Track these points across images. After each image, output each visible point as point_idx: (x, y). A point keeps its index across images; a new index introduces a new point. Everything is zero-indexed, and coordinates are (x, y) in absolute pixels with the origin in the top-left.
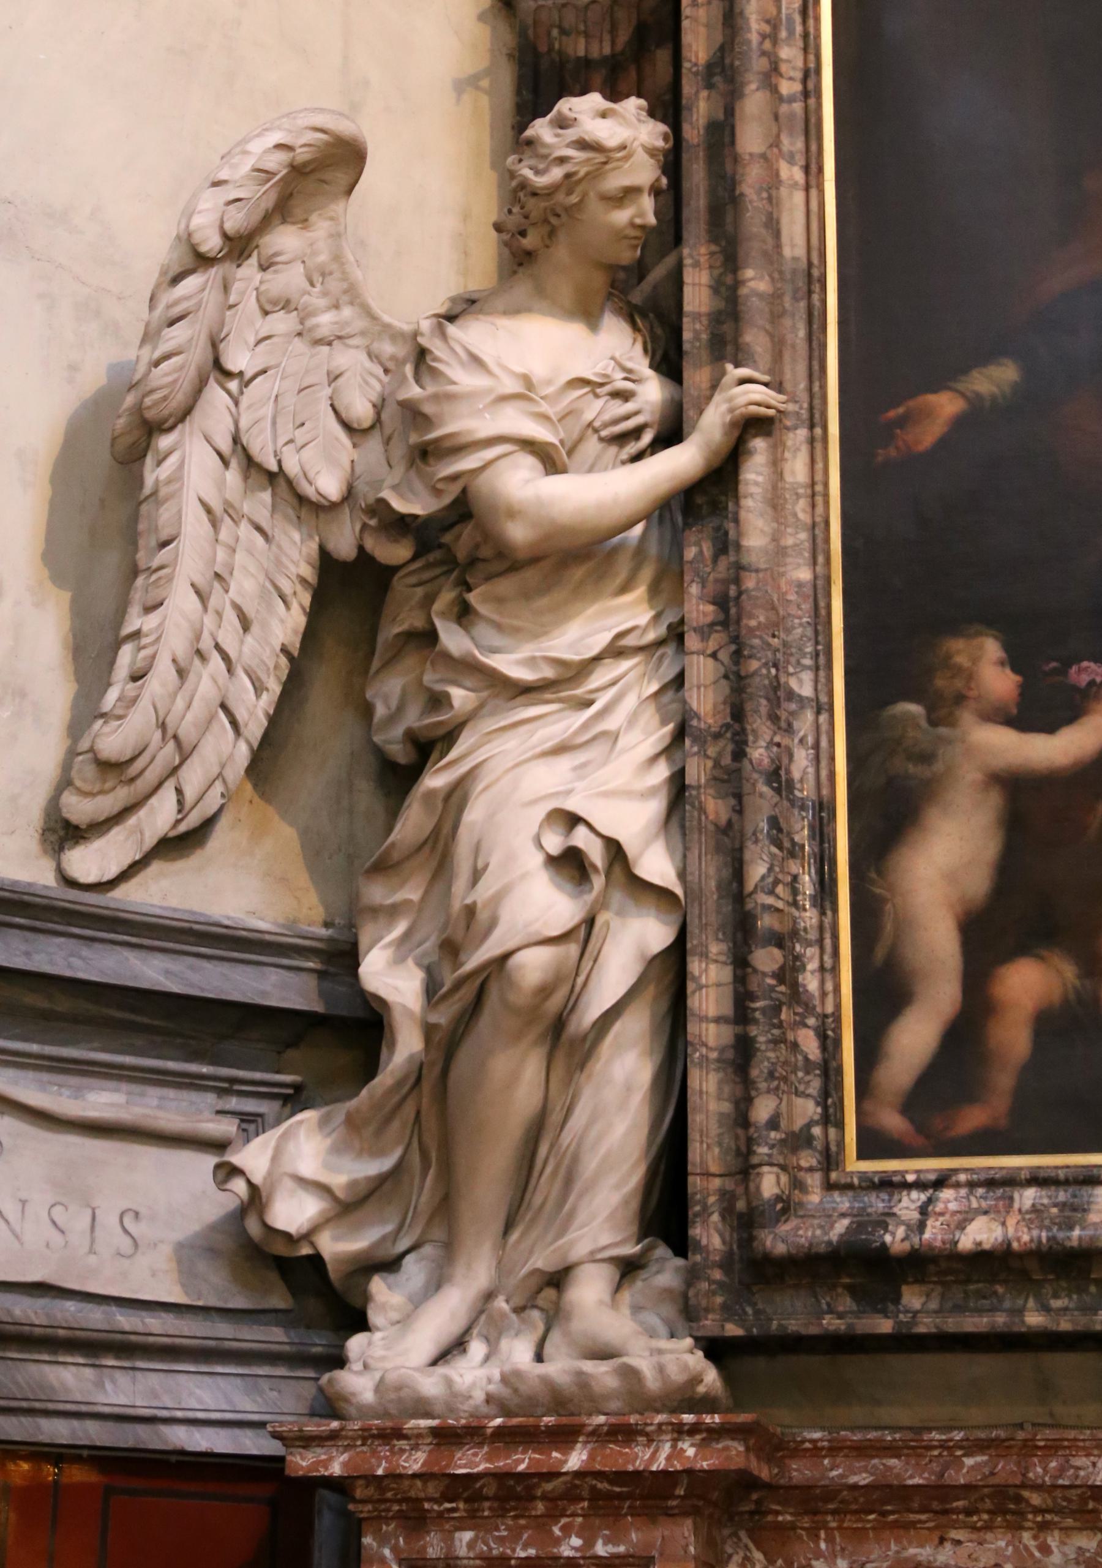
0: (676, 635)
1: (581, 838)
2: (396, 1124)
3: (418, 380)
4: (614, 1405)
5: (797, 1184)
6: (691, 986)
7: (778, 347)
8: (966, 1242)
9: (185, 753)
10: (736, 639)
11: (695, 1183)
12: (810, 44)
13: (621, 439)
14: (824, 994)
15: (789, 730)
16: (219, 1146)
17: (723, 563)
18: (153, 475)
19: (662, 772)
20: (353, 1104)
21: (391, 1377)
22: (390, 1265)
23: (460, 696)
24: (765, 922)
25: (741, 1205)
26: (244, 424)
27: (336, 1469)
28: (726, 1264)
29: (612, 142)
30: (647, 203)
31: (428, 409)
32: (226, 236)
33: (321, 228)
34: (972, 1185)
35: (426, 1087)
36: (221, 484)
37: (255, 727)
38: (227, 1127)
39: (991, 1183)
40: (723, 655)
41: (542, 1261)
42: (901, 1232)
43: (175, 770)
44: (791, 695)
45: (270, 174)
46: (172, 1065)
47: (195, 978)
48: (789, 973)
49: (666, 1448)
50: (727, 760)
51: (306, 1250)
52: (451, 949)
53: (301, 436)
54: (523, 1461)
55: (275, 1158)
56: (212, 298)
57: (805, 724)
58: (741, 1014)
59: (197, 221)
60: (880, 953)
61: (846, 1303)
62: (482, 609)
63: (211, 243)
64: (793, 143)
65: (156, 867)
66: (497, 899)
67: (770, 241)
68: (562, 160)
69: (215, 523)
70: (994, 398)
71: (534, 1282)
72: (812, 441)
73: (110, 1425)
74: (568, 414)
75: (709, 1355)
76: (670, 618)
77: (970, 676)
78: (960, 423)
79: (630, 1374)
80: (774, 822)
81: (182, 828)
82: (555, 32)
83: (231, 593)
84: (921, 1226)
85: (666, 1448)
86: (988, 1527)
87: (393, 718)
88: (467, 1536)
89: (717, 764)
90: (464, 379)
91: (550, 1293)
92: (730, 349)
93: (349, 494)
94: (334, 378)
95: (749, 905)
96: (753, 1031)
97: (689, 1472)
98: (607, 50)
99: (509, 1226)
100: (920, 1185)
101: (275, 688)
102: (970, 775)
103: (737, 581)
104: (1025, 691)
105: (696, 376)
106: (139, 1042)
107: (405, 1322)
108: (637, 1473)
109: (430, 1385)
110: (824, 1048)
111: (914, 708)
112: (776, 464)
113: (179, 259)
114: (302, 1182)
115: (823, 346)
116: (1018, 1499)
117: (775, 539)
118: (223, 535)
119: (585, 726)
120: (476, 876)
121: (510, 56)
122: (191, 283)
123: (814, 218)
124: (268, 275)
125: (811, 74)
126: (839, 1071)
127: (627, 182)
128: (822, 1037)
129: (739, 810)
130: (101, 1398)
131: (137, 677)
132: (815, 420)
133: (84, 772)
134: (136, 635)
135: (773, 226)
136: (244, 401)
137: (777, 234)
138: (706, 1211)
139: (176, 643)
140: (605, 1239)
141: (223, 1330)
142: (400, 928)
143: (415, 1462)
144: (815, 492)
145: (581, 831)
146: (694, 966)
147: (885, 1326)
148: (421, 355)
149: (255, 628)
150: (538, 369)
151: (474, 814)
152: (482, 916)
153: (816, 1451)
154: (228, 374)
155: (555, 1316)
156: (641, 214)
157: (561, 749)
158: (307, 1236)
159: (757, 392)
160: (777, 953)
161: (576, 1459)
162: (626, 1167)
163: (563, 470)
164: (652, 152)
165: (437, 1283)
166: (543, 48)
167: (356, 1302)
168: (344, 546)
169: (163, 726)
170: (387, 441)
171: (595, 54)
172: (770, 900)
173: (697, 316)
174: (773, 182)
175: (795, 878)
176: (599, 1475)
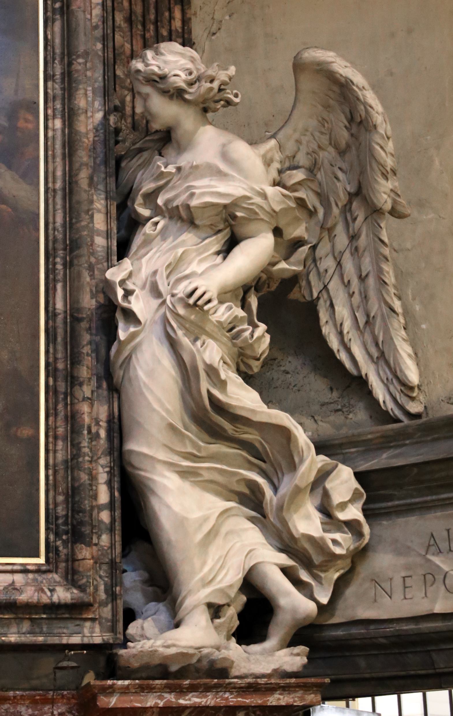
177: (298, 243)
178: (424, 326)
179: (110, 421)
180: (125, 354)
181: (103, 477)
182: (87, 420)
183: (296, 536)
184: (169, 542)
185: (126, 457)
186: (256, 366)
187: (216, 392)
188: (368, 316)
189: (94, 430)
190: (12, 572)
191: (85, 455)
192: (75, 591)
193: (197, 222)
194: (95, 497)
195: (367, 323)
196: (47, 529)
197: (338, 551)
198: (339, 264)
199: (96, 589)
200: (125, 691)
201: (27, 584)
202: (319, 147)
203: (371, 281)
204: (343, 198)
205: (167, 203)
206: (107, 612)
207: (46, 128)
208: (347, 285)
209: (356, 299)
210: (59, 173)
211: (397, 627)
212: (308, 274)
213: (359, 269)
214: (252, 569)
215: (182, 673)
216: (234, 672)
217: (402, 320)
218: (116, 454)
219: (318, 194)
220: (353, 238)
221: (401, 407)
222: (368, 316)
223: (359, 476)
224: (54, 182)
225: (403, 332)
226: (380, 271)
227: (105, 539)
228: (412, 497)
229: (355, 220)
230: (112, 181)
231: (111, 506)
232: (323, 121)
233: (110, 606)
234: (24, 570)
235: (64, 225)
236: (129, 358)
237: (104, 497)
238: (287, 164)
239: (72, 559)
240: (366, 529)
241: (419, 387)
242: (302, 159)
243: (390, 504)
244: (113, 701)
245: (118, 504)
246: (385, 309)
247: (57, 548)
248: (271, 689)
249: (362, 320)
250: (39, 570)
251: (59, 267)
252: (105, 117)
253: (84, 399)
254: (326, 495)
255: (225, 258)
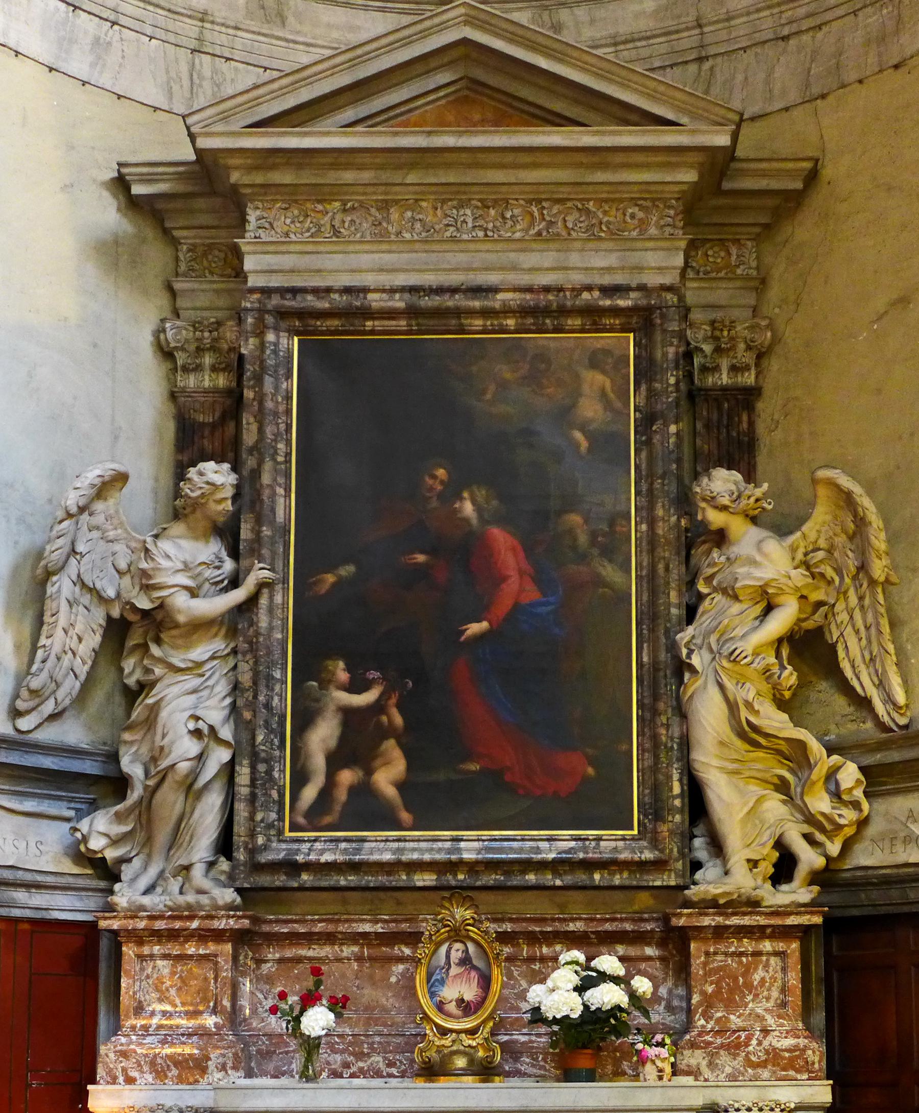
0: (234, 652)
1: (201, 724)
2: (132, 816)
3: (146, 560)
4: (207, 908)
5: (269, 840)
6: (236, 775)
7: (274, 554)
8: (323, 859)
9: (58, 685)
10: (255, 657)
11: (235, 838)
12: (288, 443)
13: (217, 583)
14: (280, 779)
15: (273, 690)
16: (68, 820)
17: (251, 630)
18: (50, 590)
19: (228, 701)
20: (118, 807)
21: (133, 898)
22: (129, 860)
23: (158, 671)
24: (263, 755)
25: (250, 846)
26: (81, 572)
27: (115, 927)
28: (244, 865)
29: (219, 483)
30: (229, 502)
31: (151, 573)
32: (79, 507)
33: (111, 502)
34: (325, 841)
35: (144, 804)
36: (74, 593)
37: (83, 677)
38: (72, 813)
39: (331, 841)
40: (251, 662)
41: (183, 861)
42: (302, 856)
43: (55, 691)
44: (273, 677)
45: (95, 485)
46: (52, 793)
47: (62, 764)
48: (269, 772)
49: (224, 921)
50: (251, 698)
51: (100, 855)
52: (154, 760)
53: (101, 575)
54: (178, 925)
55: (91, 825)
56: (72, 528)
57: (277, 688)
58: (253, 784)
59: (69, 503)
60: (299, 766)
61: (283, 878)
62: (166, 640)
63: (74, 510)
64: (281, 480)
65: (46, 723)
66: (172, 743)
67: (272, 516)
68: (201, 488)
69: (71, 606)
70: (346, 577)
71: (180, 868)
72: (283, 589)
73: (34, 911)
74: (199, 574)
75: (238, 893)
76: (232, 645)
77: (334, 674)
78: (334, 585)
79: (213, 899)
80: (266, 722)
81: (56, 711)
82: (192, 411)
83: (76, 631)
84: (309, 855)
85: (224, 921)
86: (325, 944)
87: (131, 673)
88: (158, 947)
89: (247, 699)
90: (164, 563)
91: (184, 872)
92: (256, 554)
93: (118, 595)
94: (114, 554)
95: (257, 749)
96: (257, 791)
97: (231, 929)
98: (211, 420)
99: (170, 849)
100: (309, 841)
101: (90, 663)
102: (332, 707)
103: (256, 637)
104: (352, 680)
105: (244, 563)
106: (42, 785)
107: (134, 880)
108: (214, 929)
109: (146, 900)
110: (279, 796)
111: (315, 683)
112: (271, 598)
113: (60, 514)
114: (100, 833)
115: (289, 555)
116: (335, 936)
117: (270, 624)
118: (74, 610)
119: (202, 684)
120: (164, 736)
121: (174, 417)
122: (65, 524)
123: (288, 508)
124: (92, 518)
125: (288, 455)
126: (284, 803)
127: (223, 496)
128: (279, 793)
129: (255, 716)
130: (31, 902)
131: (44, 662)
132: (285, 581)
133: (24, 693)
134: (44, 646)
135: (273, 510)
136: (82, 563)
137: (275, 514)
138: (239, 848)
139: (57, 649)
140: (205, 855)
141: (71, 880)
142: (134, 749)
143: (142, 924)
144: (285, 604)
145: (201, 722)
146: (237, 768)
147: (296, 885)
148: (147, 550)
149: (83, 642)
150: (189, 558)
151: (164, 714)
152: (166, 750)
153: (271, 922)
154: (76, 553)
155: (187, 879)
156: (227, 506)
157: (195, 691)
158: (101, 851)
159: (266, 573)
160: (265, 765)
161: (195, 924)
162: (211, 833)
163: (197, 597)
164: (232, 485)
165: (145, 868)
166: (187, 416)
167: (116, 872)
168: (116, 613)
169: (51, 678)
170: (132, 578)
171: (206, 421)
172: (264, 748)
173: (245, 540)
174: (274, 494)
175: (272, 740)
176: (202, 930)
177: (820, 604)
178: (913, 661)
179: (681, 738)
180: (689, 693)
181: (676, 776)
182: (664, 739)
183: (813, 812)
184: (719, 820)
185: (691, 762)
186: (787, 694)
187: (752, 719)
188: (871, 654)
189: (669, 745)
190: (615, 840)
191: (663, 763)
192: (657, 852)
193: (741, 598)
194: (671, 789)
195: (871, 659)
196: (639, 811)
197: (842, 821)
198: (851, 617)
199: (671, 850)
200: (689, 915)
201: (625, 848)
202: (835, 535)
203: (873, 631)
204: (853, 570)
205: (720, 583)
206: (679, 865)
207: (636, 531)
208: (857, 632)
209: (864, 642)
210: (645, 564)
211: (884, 871)
212: (830, 624)
213: (865, 621)
214: (781, 836)
215: (729, 904)
216: (765, 904)
217: (894, 658)
218: (685, 760)
219: (835, 569)
220: (861, 598)
221: (894, 720)
222: (871, 654)
223: (862, 769)
224: (641, 571)
225: (895, 667)
226: (878, 624)
227: (678, 818)
228: (899, 783)
229: (861, 586)
230: (683, 569)
231: (681, 795)
232: (835, 517)
233: (681, 862)
234: (623, 839)
235: (648, 601)
236: (691, 697)
237: (677, 789)
238: (811, 548)
239: (655, 832)
240: (865, 806)
241: (907, 706)
242: (822, 543)
243: (884, 788)
244: (682, 922)
245: (686, 794)
246: (882, 651)
247: (645, 825)
248: (790, 914)
249: (867, 657)
250: (633, 839)
251: (645, 632)
252: (679, 520)
253: (662, 725)
254: (837, 784)
255: (761, 621)
